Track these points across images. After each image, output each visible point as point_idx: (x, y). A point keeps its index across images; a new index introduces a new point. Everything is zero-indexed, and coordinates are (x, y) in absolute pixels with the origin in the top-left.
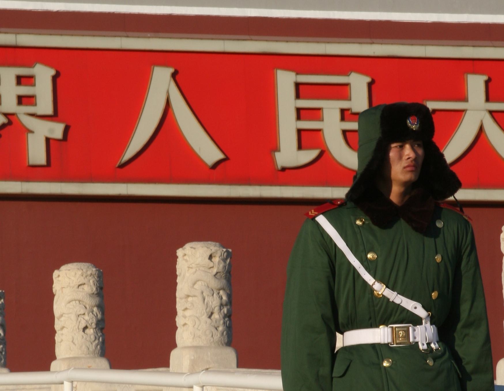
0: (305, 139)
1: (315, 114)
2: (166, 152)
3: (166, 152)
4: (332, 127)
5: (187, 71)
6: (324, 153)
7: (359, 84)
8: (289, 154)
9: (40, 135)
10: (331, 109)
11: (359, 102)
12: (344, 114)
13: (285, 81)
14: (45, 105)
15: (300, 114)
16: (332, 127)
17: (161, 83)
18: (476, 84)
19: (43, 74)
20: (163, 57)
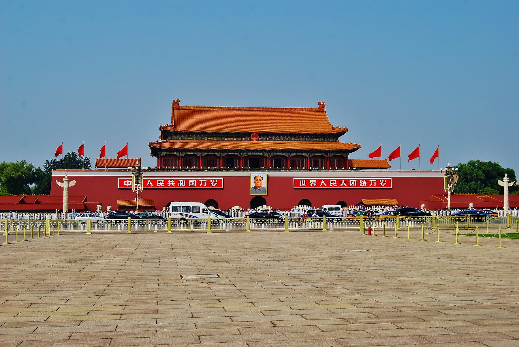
2: (323, 185)
3: (323, 185)
4: (334, 184)
8: (331, 185)
9: (315, 184)
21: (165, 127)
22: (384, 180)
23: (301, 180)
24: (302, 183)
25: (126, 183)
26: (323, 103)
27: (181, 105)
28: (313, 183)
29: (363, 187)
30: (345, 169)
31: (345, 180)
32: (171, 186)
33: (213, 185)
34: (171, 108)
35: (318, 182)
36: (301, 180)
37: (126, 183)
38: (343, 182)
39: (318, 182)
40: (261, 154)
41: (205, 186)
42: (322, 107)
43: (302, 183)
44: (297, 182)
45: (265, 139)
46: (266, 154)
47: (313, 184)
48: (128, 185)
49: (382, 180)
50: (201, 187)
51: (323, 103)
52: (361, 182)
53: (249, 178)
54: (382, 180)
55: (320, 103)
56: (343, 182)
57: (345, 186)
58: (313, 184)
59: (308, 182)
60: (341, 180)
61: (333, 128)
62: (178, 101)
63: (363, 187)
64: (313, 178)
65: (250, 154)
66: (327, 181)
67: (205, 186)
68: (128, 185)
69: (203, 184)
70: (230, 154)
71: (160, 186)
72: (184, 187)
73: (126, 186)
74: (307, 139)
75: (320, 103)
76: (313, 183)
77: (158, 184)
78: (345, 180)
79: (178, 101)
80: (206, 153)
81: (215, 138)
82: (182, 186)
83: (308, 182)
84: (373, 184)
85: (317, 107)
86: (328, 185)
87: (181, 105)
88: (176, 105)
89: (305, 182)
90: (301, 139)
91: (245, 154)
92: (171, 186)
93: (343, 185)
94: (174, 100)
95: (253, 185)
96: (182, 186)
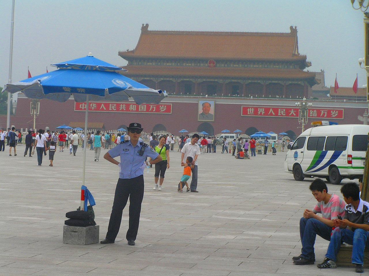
0: (280, 113)
1: (281, 112)
2: (271, 114)
4: (282, 112)
5: (273, 109)
6: (282, 114)
7: (284, 110)
9: (263, 113)
10: (282, 111)
11: (284, 111)
12: (283, 112)
13: (279, 110)
14: (263, 111)
15: (280, 112)
16: (282, 112)
17: (271, 110)
18: (292, 110)
19: (263, 109)
20: (271, 108)
21: (125, 53)
22: (336, 111)
23: (249, 108)
24: (250, 111)
25: (82, 106)
26: (296, 27)
27: (149, 29)
28: (261, 111)
29: (312, 117)
30: (286, 97)
31: (295, 110)
32: (123, 110)
33: (162, 111)
34: (140, 32)
35: (267, 110)
36: (249, 108)
37: (82, 106)
38: (292, 112)
39: (267, 110)
40: (216, 80)
41: (154, 111)
42: (294, 31)
43: (250, 111)
44: (245, 109)
45: (223, 65)
46: (221, 81)
47: (261, 113)
48: (83, 108)
49: (333, 111)
50: (150, 112)
51: (296, 27)
52: (311, 112)
53: (197, 105)
54: (333, 111)
55: (291, 28)
56: (292, 112)
57: (294, 116)
58: (261, 113)
59: (256, 110)
60: (291, 109)
61: (295, 55)
62: (147, 25)
63: (312, 117)
64: (261, 107)
65: (204, 80)
66: (276, 110)
67: (154, 111)
68: (83, 108)
69: (153, 109)
70: (185, 79)
71: (113, 110)
72: (134, 111)
73: (81, 109)
74: (266, 66)
75: (291, 28)
76: (261, 111)
77: (110, 107)
78: (295, 110)
79: (147, 25)
80: (162, 79)
81: (173, 64)
82: (132, 111)
83: (256, 110)
84: (324, 114)
85: (289, 31)
86: (277, 114)
87: (149, 29)
88: (145, 28)
89: (253, 110)
90: (260, 66)
91: (199, 80)
92: (123, 110)
93: (292, 115)
94: (143, 25)
95: (200, 111)
96: (132, 111)
